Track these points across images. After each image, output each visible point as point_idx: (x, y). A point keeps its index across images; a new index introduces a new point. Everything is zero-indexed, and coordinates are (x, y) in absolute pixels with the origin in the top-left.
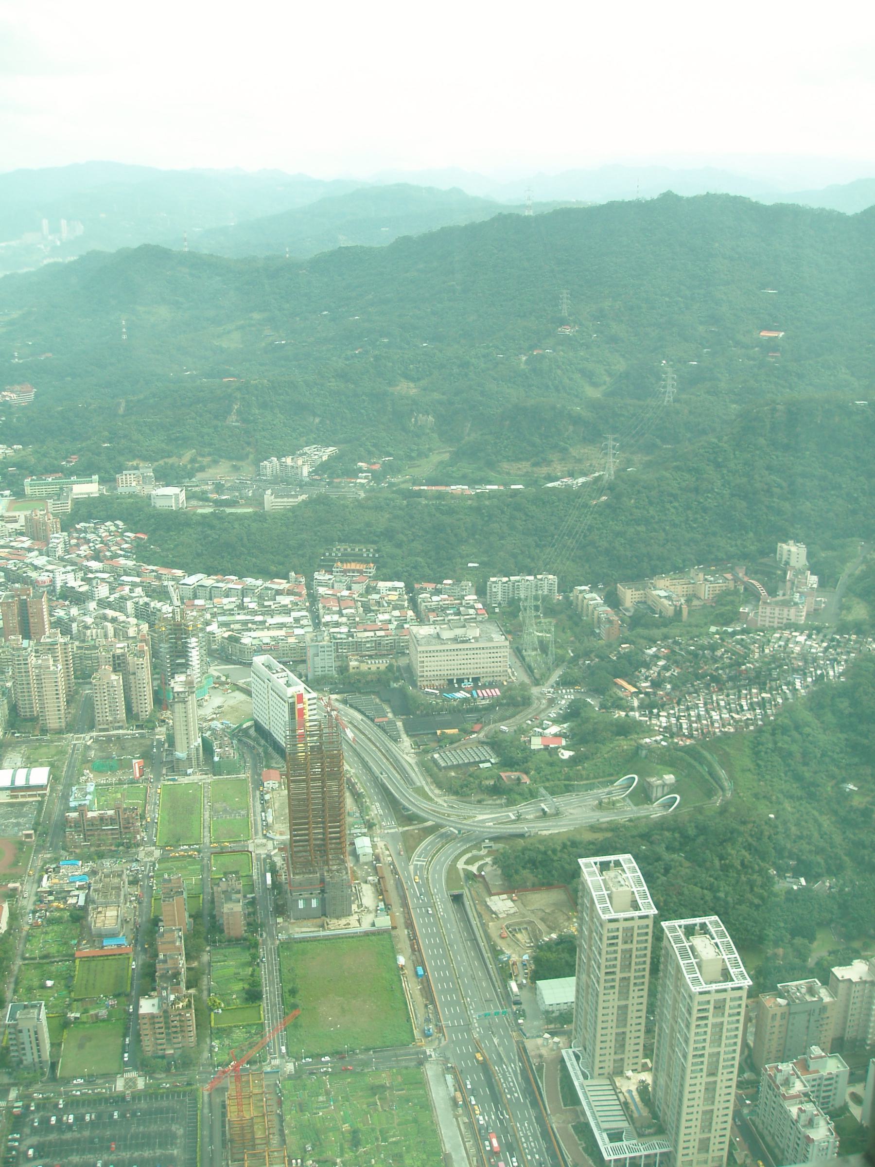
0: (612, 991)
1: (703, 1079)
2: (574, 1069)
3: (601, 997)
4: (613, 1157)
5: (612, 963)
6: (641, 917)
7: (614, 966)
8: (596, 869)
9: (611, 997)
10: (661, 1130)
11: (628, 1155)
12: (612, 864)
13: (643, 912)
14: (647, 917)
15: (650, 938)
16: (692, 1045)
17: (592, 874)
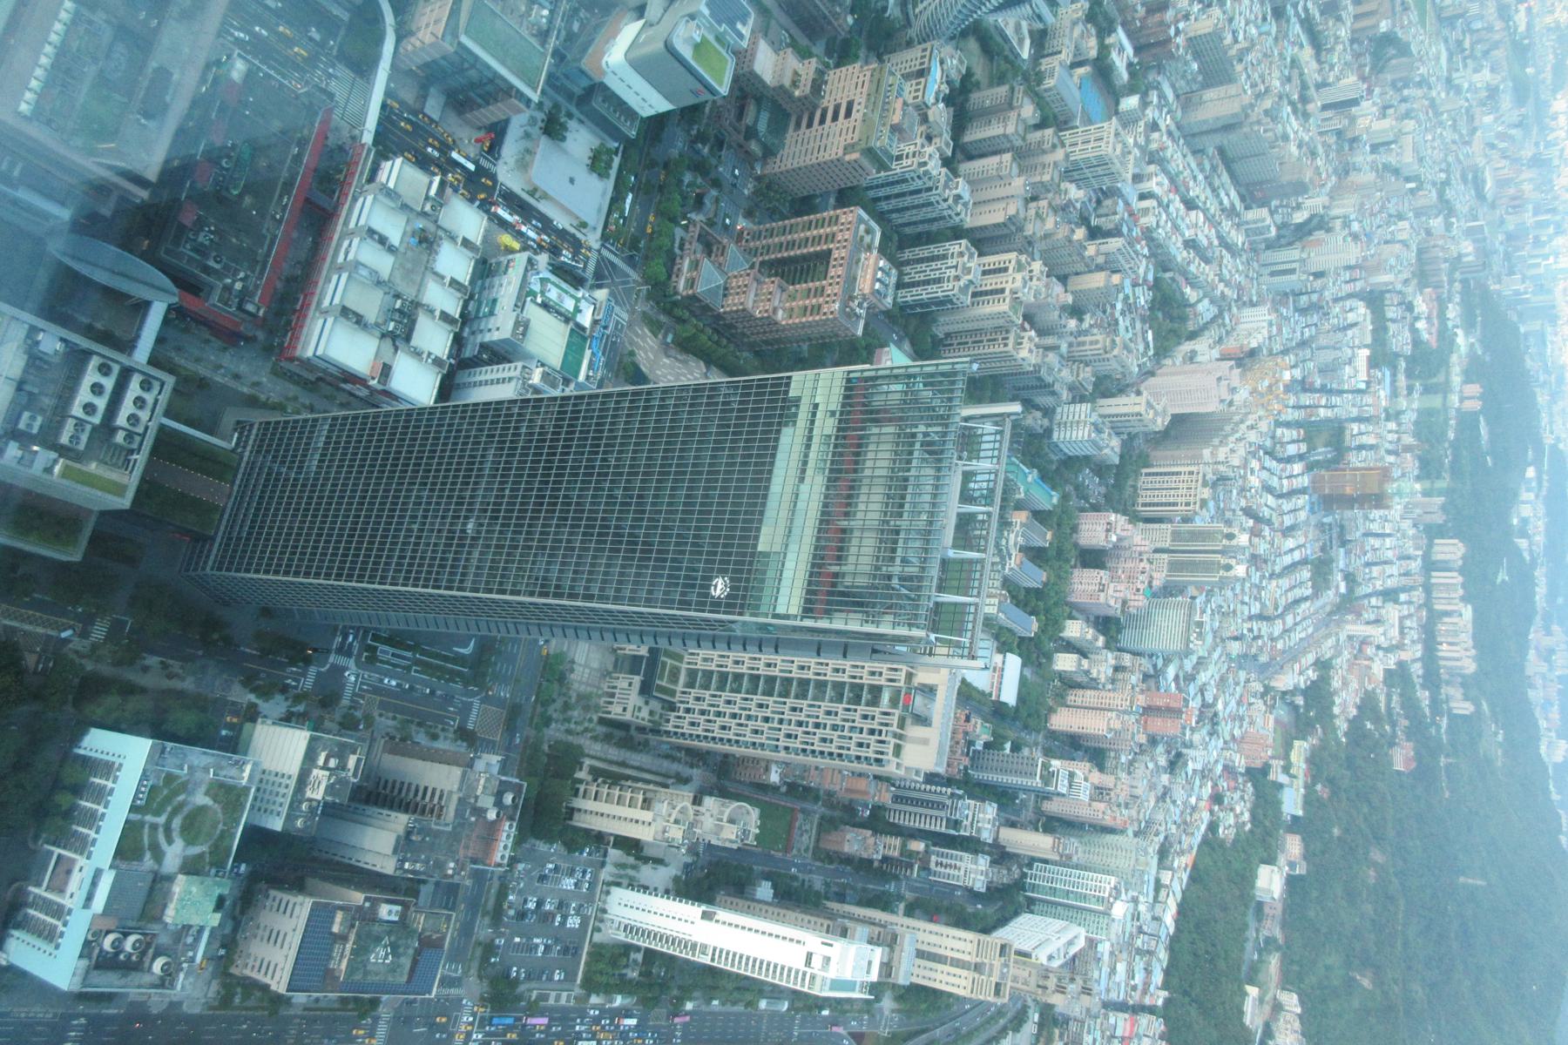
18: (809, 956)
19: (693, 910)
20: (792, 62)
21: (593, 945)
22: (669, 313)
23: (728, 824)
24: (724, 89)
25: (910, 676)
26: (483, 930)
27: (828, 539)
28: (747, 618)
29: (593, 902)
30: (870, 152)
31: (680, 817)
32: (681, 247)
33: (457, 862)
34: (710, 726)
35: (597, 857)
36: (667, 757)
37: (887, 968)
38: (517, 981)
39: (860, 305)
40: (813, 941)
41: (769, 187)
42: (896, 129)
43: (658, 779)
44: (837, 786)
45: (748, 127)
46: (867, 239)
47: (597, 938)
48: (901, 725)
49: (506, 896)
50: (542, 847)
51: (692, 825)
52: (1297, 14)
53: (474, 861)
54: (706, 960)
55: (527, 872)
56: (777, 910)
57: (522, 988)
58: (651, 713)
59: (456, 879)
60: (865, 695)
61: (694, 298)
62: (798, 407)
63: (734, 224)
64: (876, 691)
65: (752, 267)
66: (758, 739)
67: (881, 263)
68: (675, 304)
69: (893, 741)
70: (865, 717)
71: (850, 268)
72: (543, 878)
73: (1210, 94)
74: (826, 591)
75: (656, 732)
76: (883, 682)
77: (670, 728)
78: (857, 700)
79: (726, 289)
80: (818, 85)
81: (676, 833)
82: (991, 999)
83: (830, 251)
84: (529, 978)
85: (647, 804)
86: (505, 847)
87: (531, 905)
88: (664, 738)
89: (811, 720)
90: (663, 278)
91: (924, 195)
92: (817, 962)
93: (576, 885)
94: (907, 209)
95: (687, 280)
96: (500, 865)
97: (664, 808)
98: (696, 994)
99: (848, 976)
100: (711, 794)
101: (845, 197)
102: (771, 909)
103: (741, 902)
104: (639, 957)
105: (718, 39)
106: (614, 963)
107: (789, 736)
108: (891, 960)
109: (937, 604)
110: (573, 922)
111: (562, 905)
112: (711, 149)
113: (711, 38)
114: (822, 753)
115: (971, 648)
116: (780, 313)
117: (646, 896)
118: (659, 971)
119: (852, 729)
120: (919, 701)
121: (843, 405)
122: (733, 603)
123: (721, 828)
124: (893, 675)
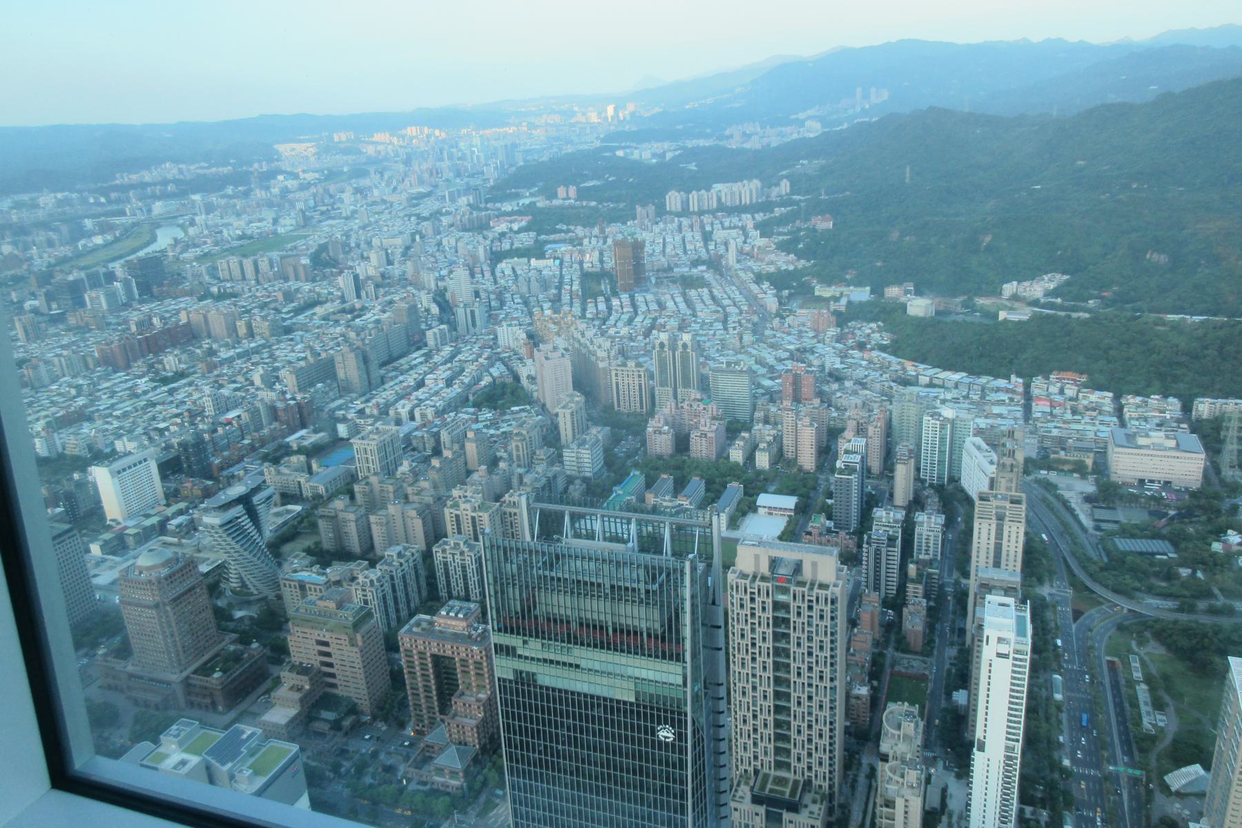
18: (999, 655)
19: (978, 758)
20: (283, 692)
22: (479, 793)
23: (902, 731)
24: (294, 748)
25: (763, 579)
27: (622, 643)
28: (689, 709)
30: (356, 626)
31: (898, 773)
32: (425, 784)
34: (821, 748)
36: (853, 787)
37: (1008, 591)
39: (476, 629)
40: (988, 652)
41: (382, 709)
42: (340, 606)
43: (872, 794)
44: (866, 635)
45: (332, 728)
46: (424, 625)
48: (802, 584)
51: (903, 762)
52: (291, 318)
54: (1019, 747)
56: (973, 686)
58: (814, 802)
60: (781, 614)
61: (467, 772)
62: (521, 672)
63: (409, 738)
64: (777, 606)
65: (443, 721)
66: (827, 705)
67: (444, 613)
68: (470, 788)
69: (816, 590)
70: (799, 614)
71: (444, 639)
73: (341, 374)
74: (663, 644)
75: (831, 797)
76: (770, 600)
77: (826, 785)
78: (786, 621)
79: (460, 743)
80: (303, 670)
81: (913, 776)
82: (1024, 507)
83: (433, 656)
85: (890, 804)
88: (836, 789)
89: (806, 659)
90: (448, 799)
91: (396, 582)
92: (1003, 649)
94: (407, 594)
95: (451, 778)
97: (892, 787)
98: (1056, 755)
99: (1011, 622)
100: (878, 746)
101: (392, 645)
102: (973, 692)
103: (970, 718)
105: (252, 755)
107: (821, 678)
108: (1001, 588)
109: (673, 555)
112: (347, 759)
113: (252, 760)
114: (832, 649)
115: (704, 527)
116: (481, 696)
117: (973, 803)
118: (1039, 791)
119: (810, 624)
120: (782, 571)
121: (518, 634)
122: (677, 721)
123: (906, 737)
124: (764, 592)
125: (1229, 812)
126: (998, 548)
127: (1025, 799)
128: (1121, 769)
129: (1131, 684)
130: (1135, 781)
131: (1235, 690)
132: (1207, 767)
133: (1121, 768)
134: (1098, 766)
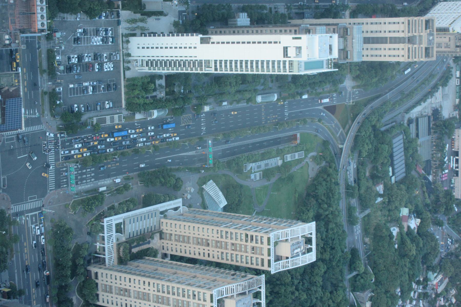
0: (219, 236)
1: (152, 291)
2: (168, 205)
3: (216, 228)
4: (105, 224)
5: (239, 237)
6: (269, 261)
7: (236, 239)
8: (306, 233)
9: (215, 235)
10: (121, 261)
11: (106, 235)
12: (309, 246)
13: (272, 263)
14: (269, 266)
15: (254, 266)
16: (176, 286)
17: (303, 230)
18: (285, 49)
19: (194, 39)
21: (128, 80)
26: (45, 84)
29: (119, 51)
33: (10, 34)
35: (113, 18)
37: (344, 52)
38: (79, 114)
40: (286, 39)
47: (129, 74)
49: (54, 57)
50: (70, 18)
53: (23, 32)
55: (65, 38)
56: (255, 29)
57: (84, 118)
59: (13, 47)
72: (77, 40)
82: (424, 59)
84: (87, 109)
86: (42, 17)
87: (74, 61)
92: (292, 52)
93: (102, 40)
96: (43, 31)
98: (209, 100)
99: (316, 57)
102: (250, 30)
103: (227, 30)
104: (163, 82)
106: (145, 89)
108: (346, 46)
110: (108, 67)
111: (96, 57)
117: (157, 38)
118: (179, 89)
125: (197, 226)
126: (383, 40)
127: (170, 78)
128: (211, 150)
129: (280, 153)
130: (204, 159)
131: (290, 226)
132: (225, 209)
133: (211, 149)
134: (209, 132)
